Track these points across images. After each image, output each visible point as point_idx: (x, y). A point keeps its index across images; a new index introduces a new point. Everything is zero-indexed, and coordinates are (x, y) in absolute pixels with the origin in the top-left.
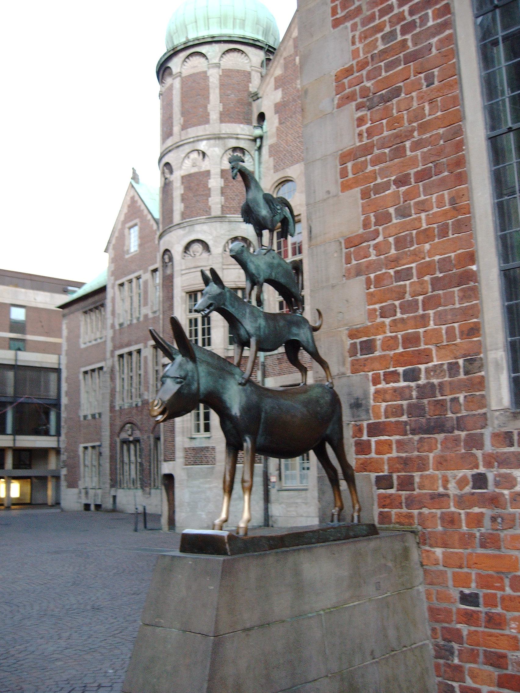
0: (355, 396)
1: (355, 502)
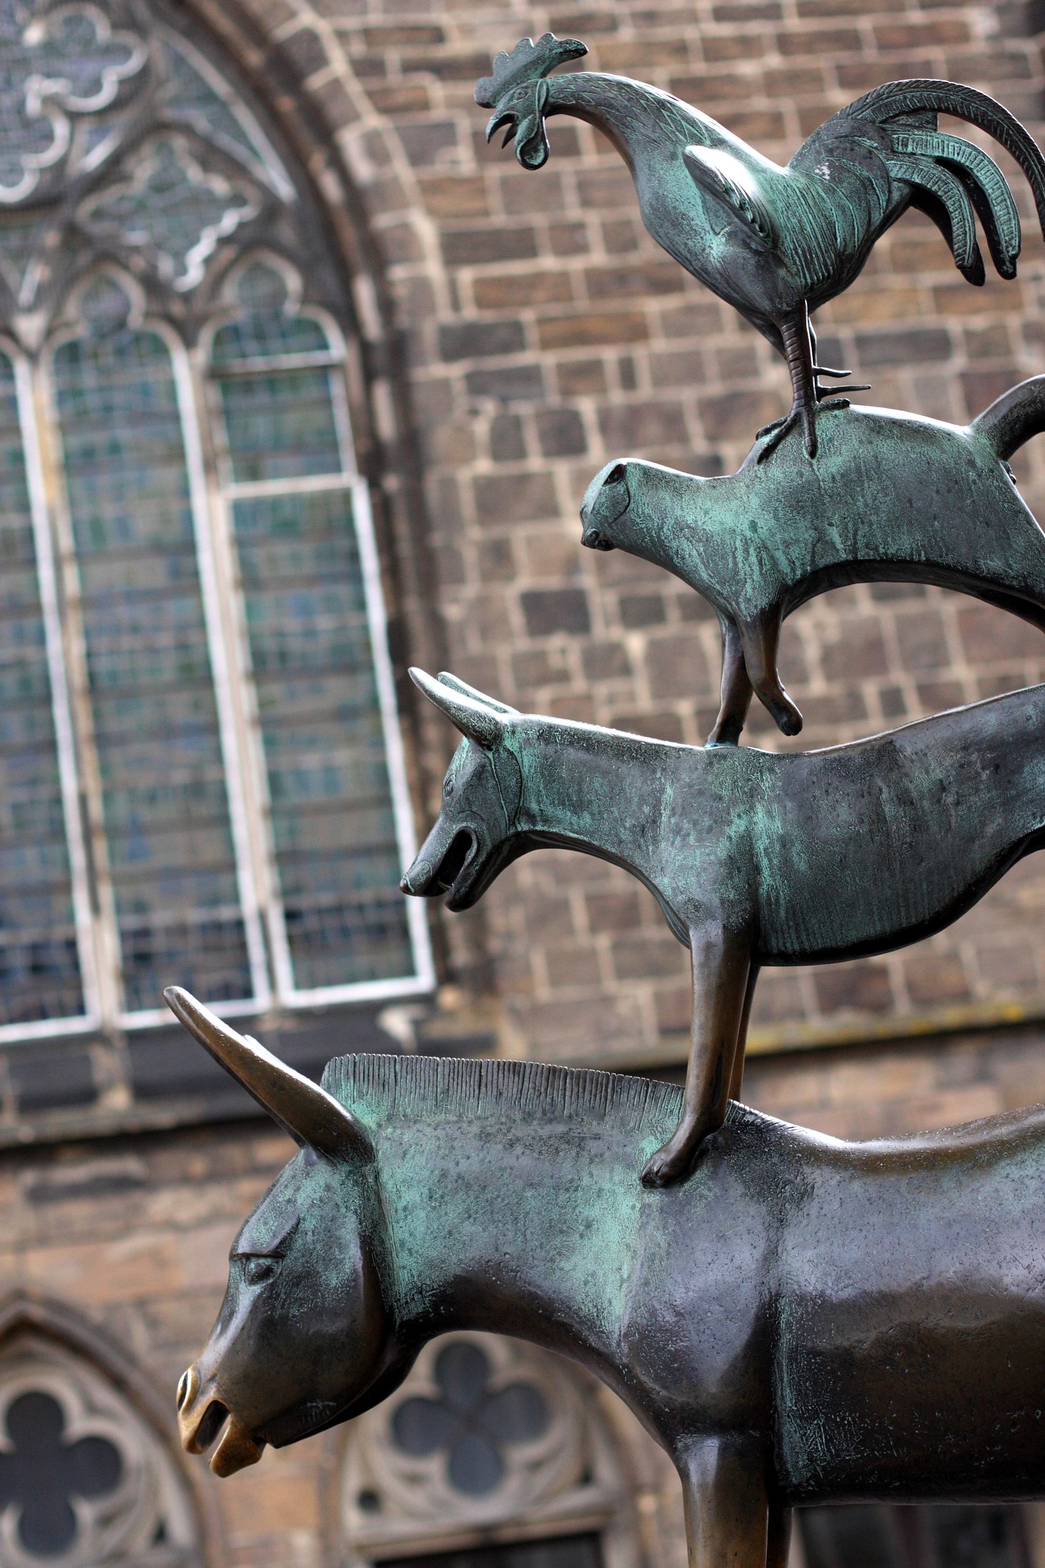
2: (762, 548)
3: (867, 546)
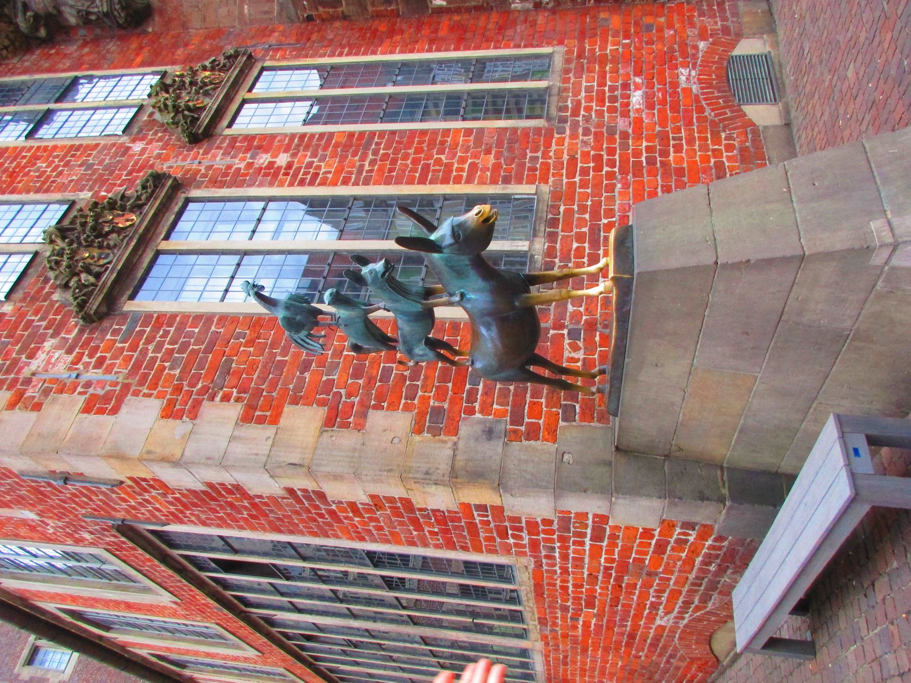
0: (480, 433)
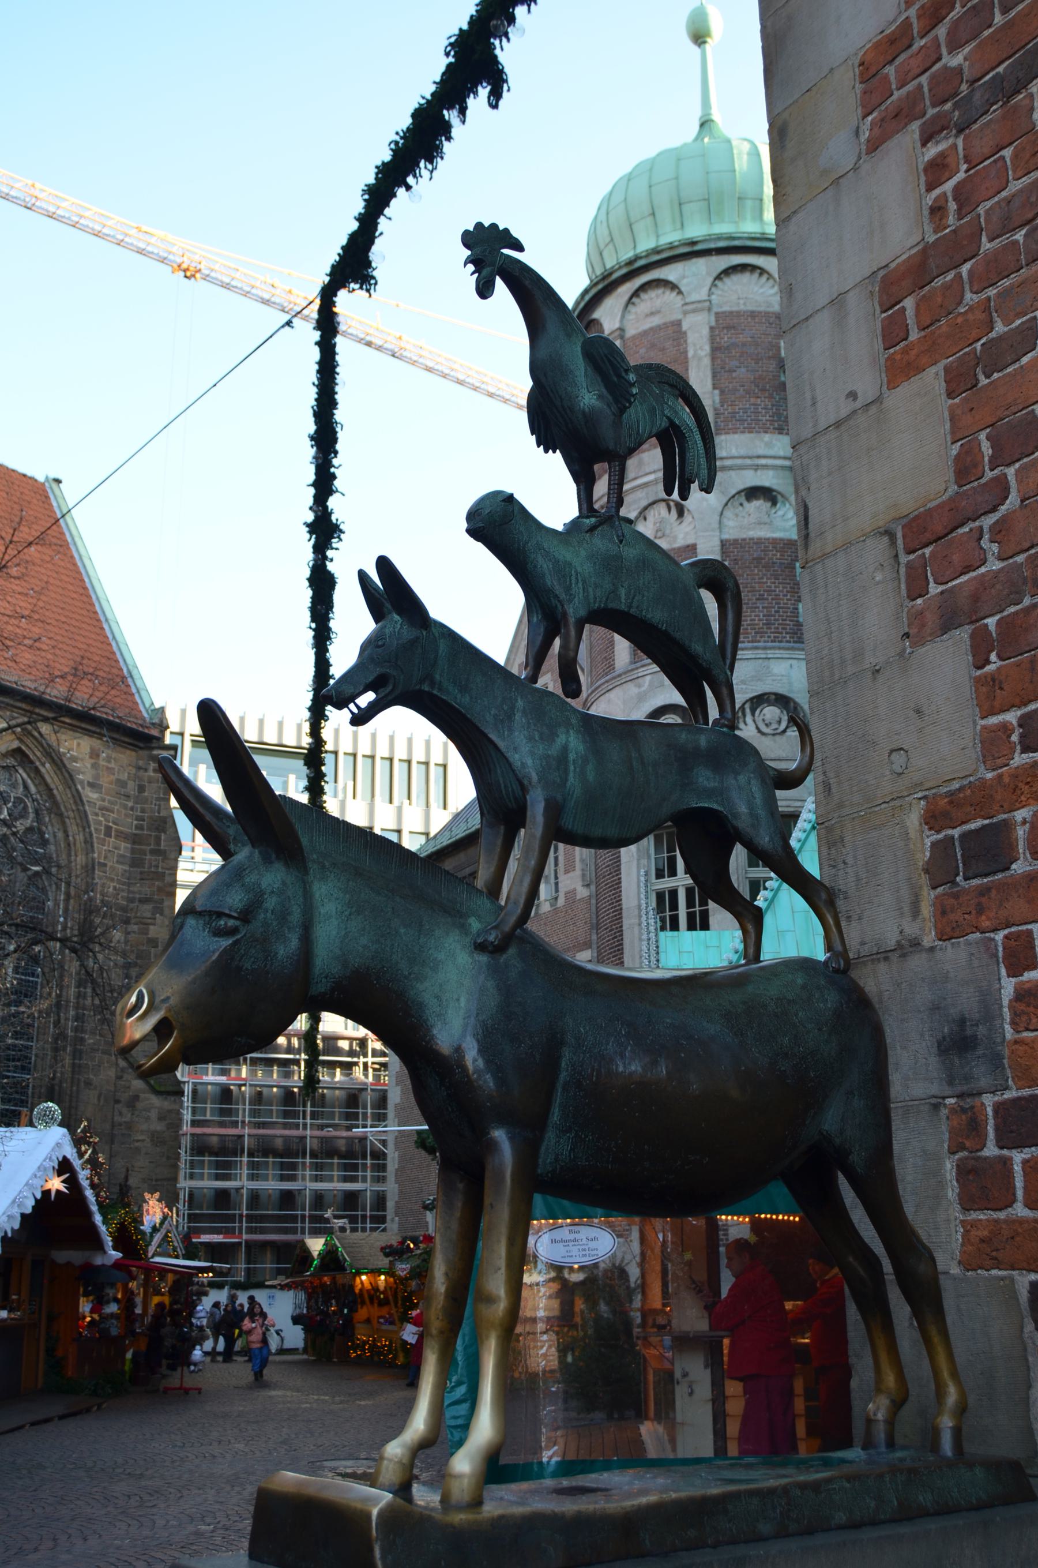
1: (946, 1374)
2: (584, 582)
3: (637, 607)
